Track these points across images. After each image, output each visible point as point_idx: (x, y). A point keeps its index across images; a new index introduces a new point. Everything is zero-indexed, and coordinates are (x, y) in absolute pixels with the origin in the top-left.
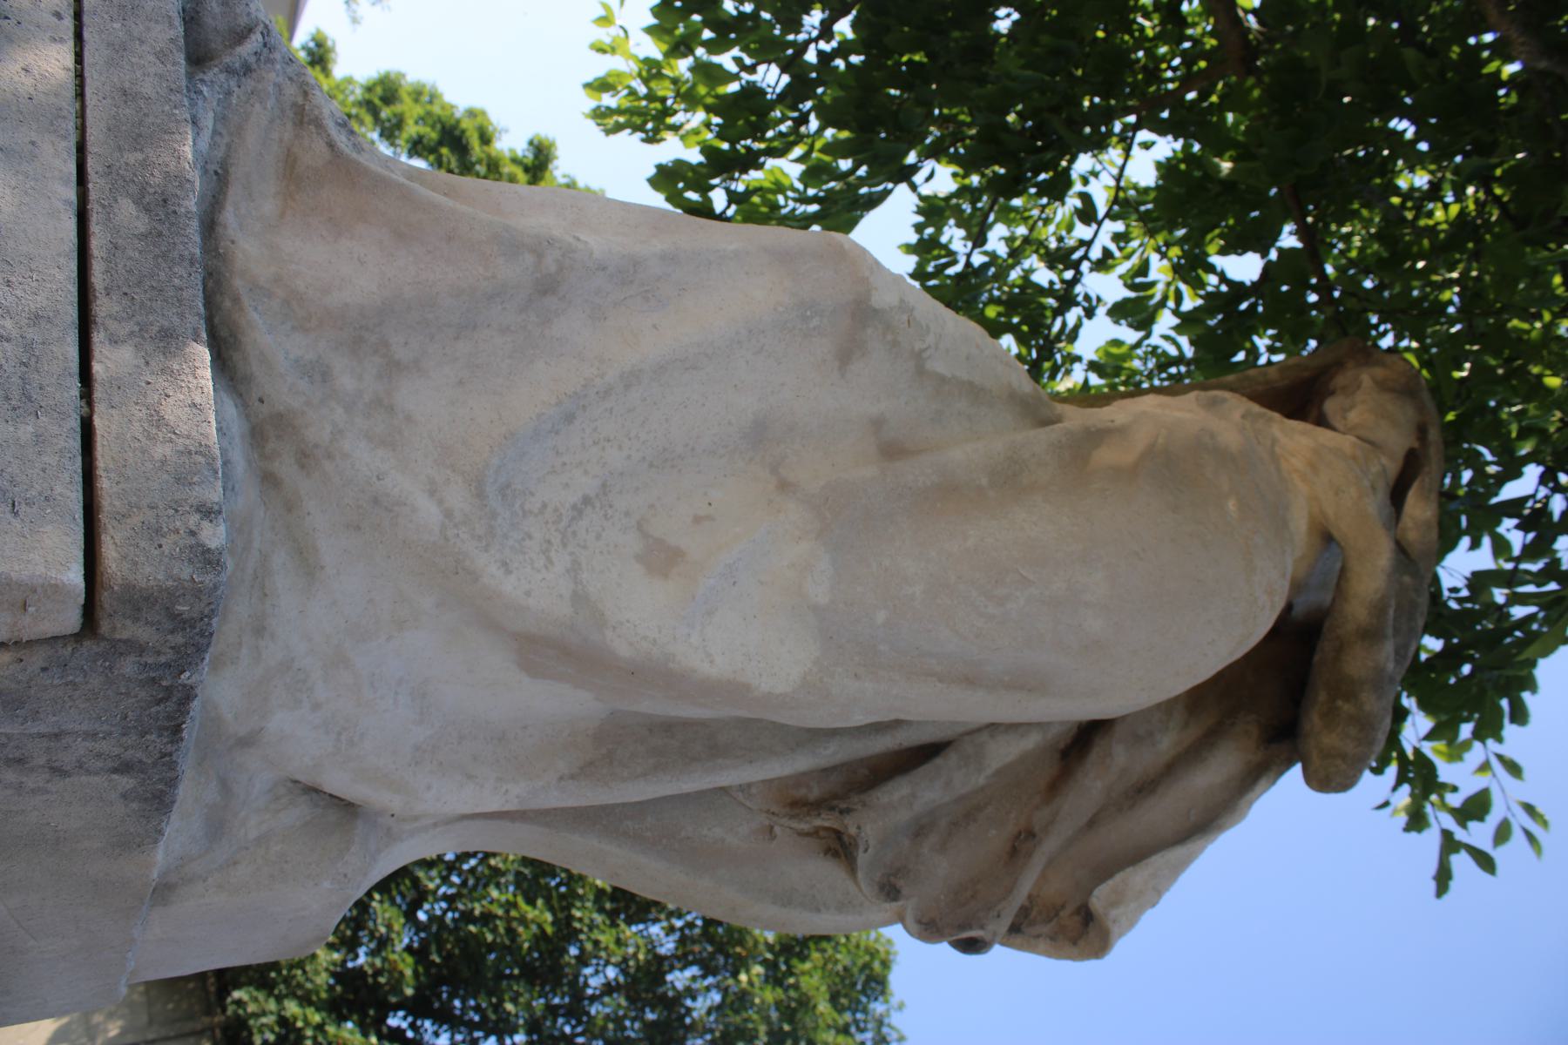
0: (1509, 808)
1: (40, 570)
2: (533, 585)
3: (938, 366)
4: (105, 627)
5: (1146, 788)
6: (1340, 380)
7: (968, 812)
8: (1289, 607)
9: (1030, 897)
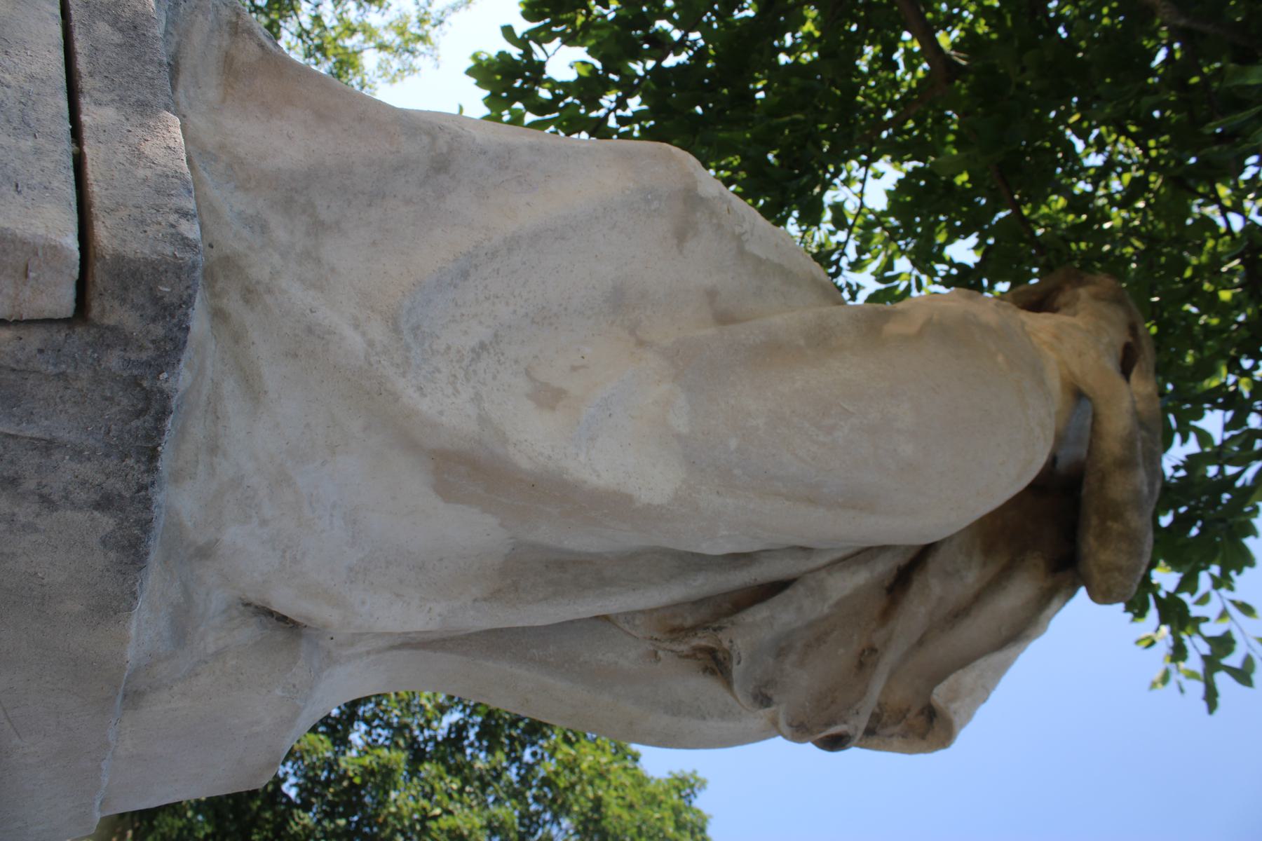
0: (1249, 645)
1: (41, 231)
2: (446, 407)
4: (95, 312)
5: (960, 613)
6: (1062, 299)
7: (817, 636)
8: (1053, 460)
9: (879, 705)
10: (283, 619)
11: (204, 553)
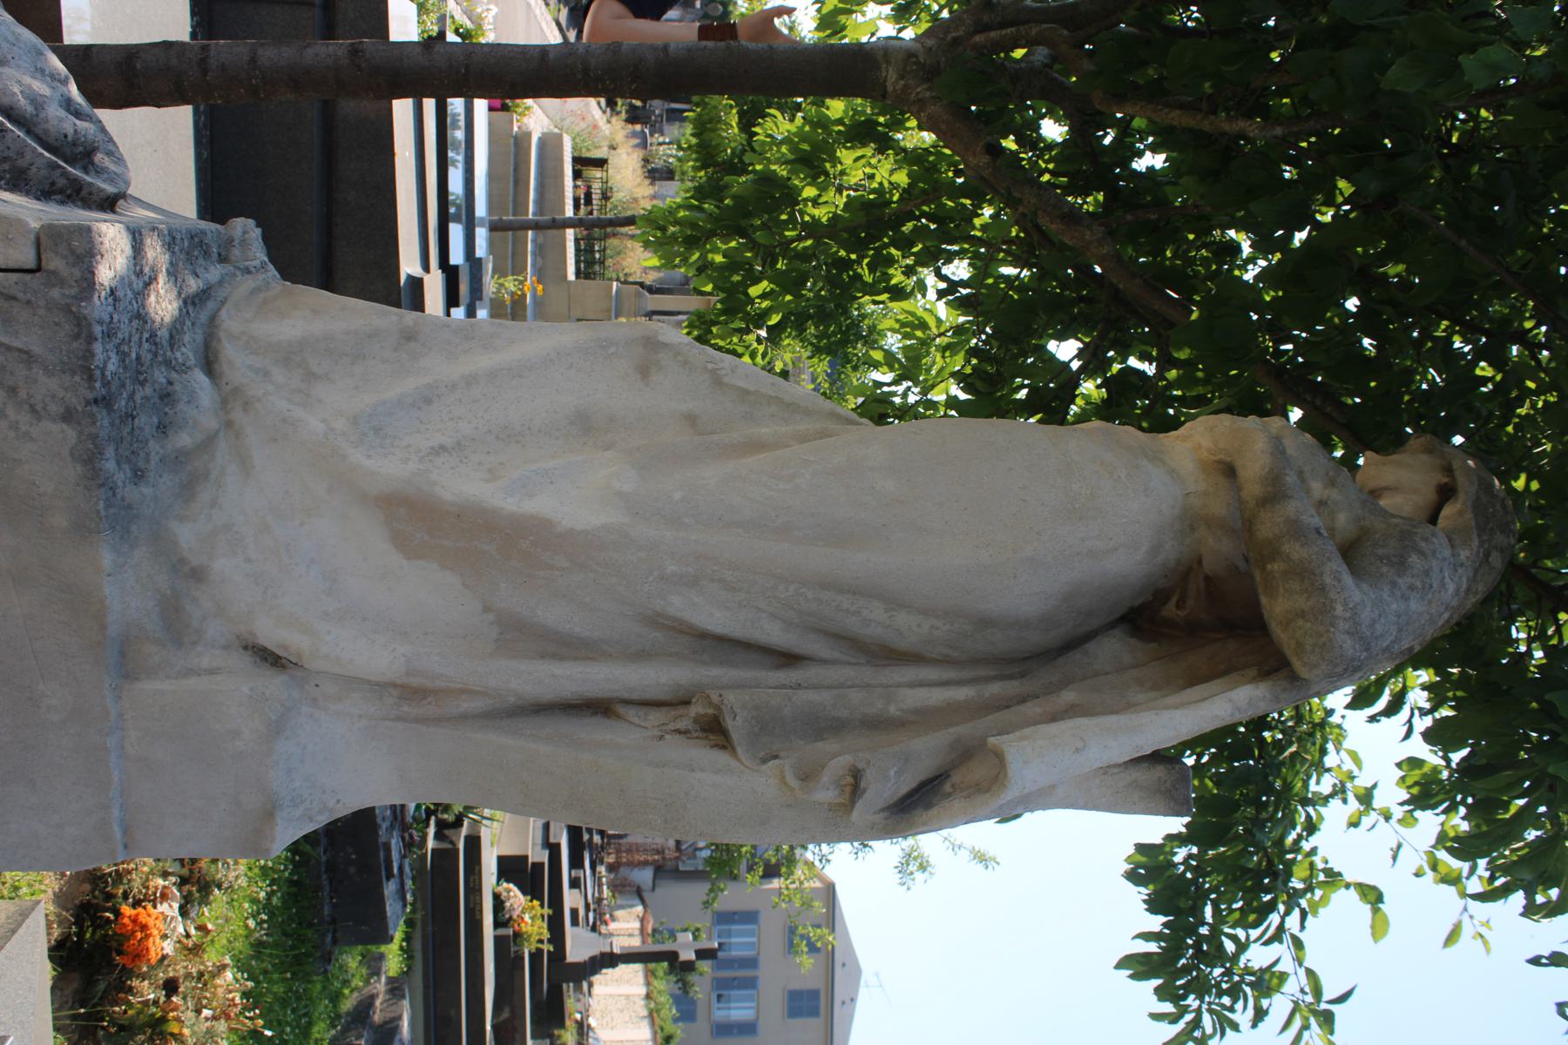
2: (391, 467)
3: (741, 384)
10: (271, 659)
11: (198, 575)
